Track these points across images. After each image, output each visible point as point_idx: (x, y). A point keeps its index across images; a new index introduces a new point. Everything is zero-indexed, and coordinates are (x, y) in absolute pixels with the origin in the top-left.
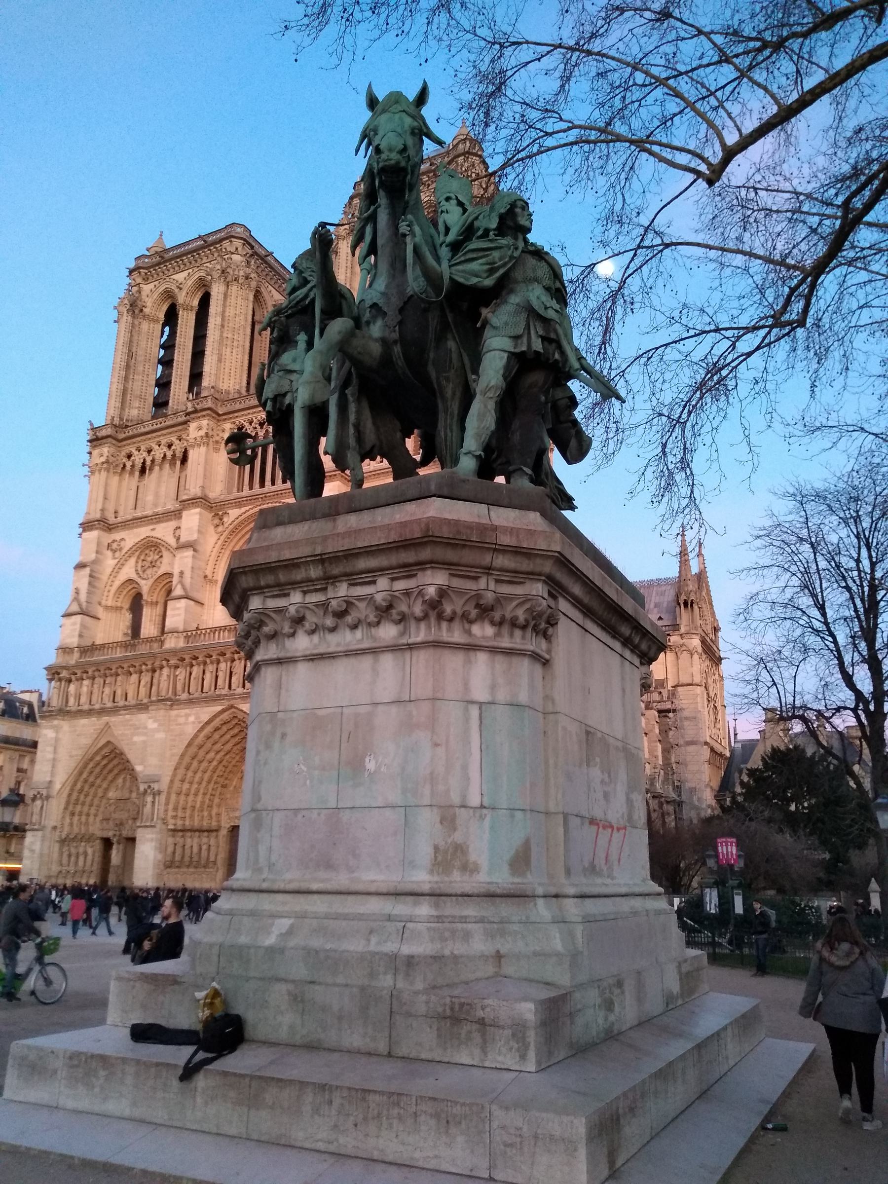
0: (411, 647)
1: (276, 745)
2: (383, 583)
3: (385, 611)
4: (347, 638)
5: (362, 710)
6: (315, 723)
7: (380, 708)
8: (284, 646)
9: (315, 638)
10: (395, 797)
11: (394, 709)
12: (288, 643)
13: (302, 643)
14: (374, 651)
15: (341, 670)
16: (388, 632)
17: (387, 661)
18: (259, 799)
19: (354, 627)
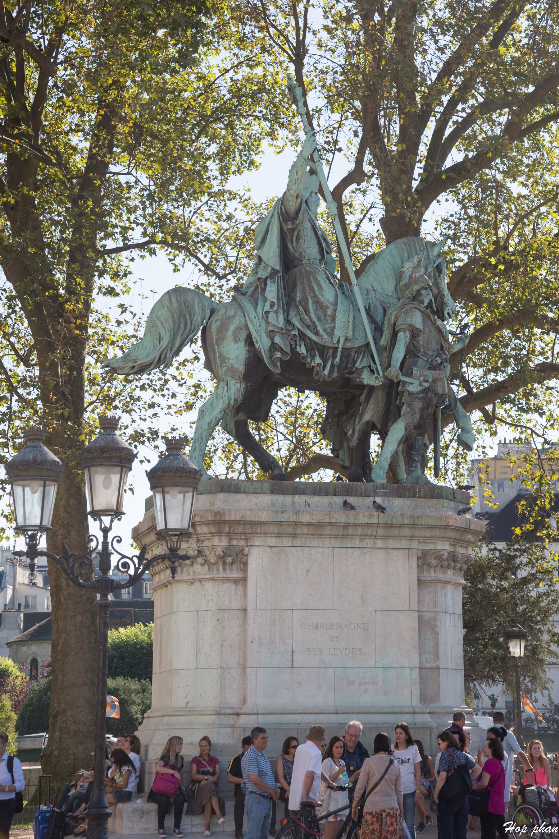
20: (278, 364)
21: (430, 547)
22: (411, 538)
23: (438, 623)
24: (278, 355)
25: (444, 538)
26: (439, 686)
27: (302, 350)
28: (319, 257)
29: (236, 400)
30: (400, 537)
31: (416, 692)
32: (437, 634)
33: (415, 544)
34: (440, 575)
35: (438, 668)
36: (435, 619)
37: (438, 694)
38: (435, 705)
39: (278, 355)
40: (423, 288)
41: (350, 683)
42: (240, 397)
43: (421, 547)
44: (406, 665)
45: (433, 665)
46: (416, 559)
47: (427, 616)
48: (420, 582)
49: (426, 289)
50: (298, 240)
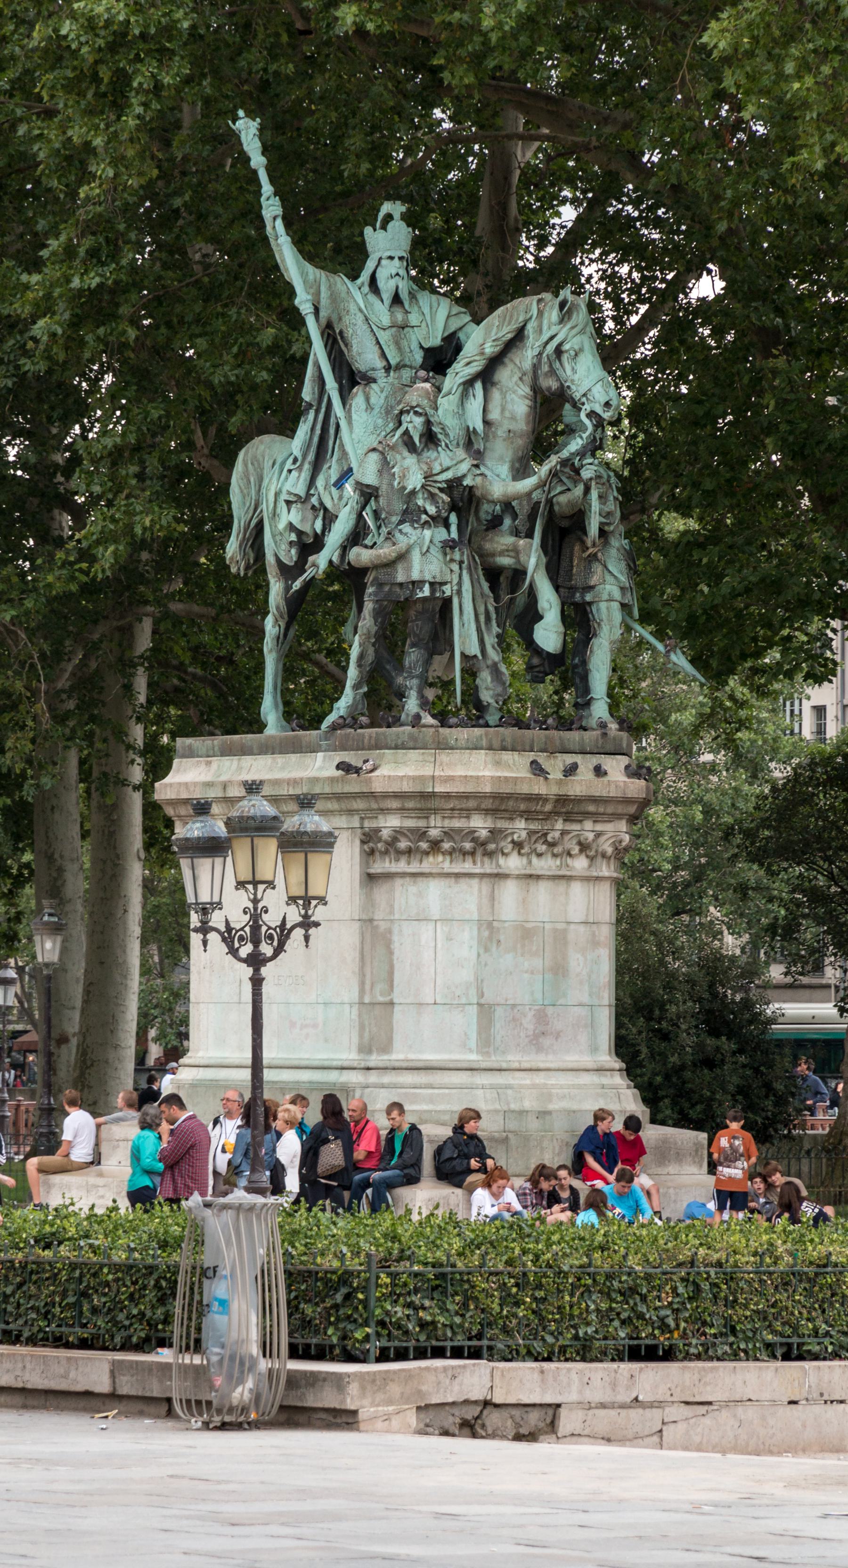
0: (598, 878)
1: (494, 949)
2: (588, 825)
3: (584, 847)
4: (546, 865)
5: (560, 926)
6: (526, 933)
7: (572, 926)
8: (498, 866)
9: (525, 860)
10: (586, 999)
11: (582, 928)
12: (502, 861)
13: (513, 863)
14: (569, 878)
15: (543, 890)
16: (580, 864)
17: (577, 888)
18: (482, 995)
19: (555, 856)
20: (293, 551)
21: (374, 824)
22: (350, 812)
23: (395, 938)
24: (293, 537)
25: (383, 811)
26: (391, 1030)
27: (318, 526)
28: (380, 364)
29: (278, 608)
30: (341, 812)
31: (355, 1040)
32: (391, 953)
33: (356, 822)
34: (401, 866)
35: (392, 1003)
36: (390, 931)
37: (390, 1040)
38: (386, 1057)
39: (293, 537)
40: (402, 412)
41: (293, 1025)
42: (282, 603)
43: (367, 824)
44: (346, 1000)
45: (387, 999)
46: (357, 842)
47: (383, 926)
48: (371, 879)
49: (408, 412)
50: (346, 345)
